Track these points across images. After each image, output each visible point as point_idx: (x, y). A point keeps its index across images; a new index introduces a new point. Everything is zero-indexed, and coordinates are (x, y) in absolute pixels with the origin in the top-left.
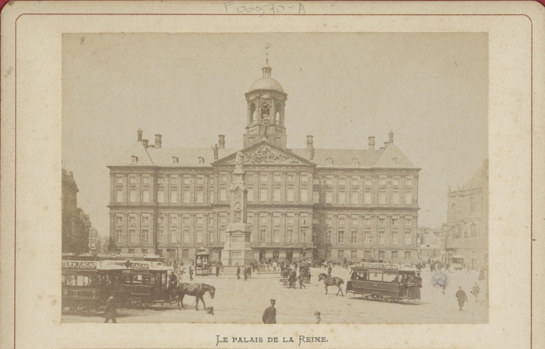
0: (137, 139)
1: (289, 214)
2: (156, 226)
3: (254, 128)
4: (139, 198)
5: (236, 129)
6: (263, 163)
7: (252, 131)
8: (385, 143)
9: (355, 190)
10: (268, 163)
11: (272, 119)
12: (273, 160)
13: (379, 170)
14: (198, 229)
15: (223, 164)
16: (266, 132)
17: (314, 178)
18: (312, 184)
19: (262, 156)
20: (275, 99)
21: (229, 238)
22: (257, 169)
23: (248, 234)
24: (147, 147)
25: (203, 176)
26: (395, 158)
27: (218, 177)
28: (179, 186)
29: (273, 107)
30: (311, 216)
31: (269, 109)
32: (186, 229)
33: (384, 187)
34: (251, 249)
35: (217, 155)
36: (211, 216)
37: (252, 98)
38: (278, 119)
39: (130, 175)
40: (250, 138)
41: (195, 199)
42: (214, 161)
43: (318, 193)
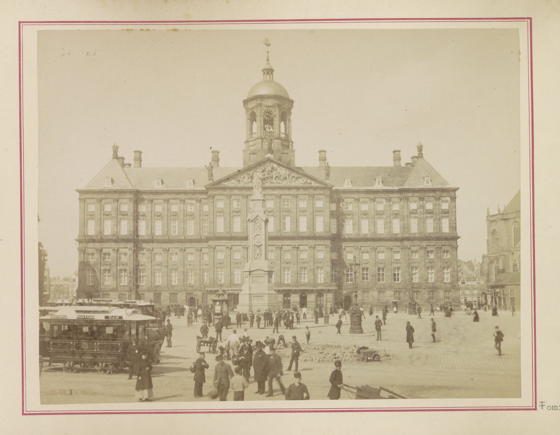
0: (111, 156)
3: (255, 142)
7: (253, 146)
9: (380, 216)
12: (280, 181)
13: (408, 191)
14: (189, 267)
15: (220, 186)
17: (332, 202)
18: (328, 211)
19: (266, 176)
20: (279, 106)
21: (247, 279)
23: (270, 273)
24: (123, 165)
25: (194, 202)
27: (213, 202)
30: (329, 249)
32: (174, 267)
33: (414, 212)
34: (275, 292)
35: (212, 175)
37: (251, 105)
38: (283, 130)
39: (104, 201)
42: (208, 182)
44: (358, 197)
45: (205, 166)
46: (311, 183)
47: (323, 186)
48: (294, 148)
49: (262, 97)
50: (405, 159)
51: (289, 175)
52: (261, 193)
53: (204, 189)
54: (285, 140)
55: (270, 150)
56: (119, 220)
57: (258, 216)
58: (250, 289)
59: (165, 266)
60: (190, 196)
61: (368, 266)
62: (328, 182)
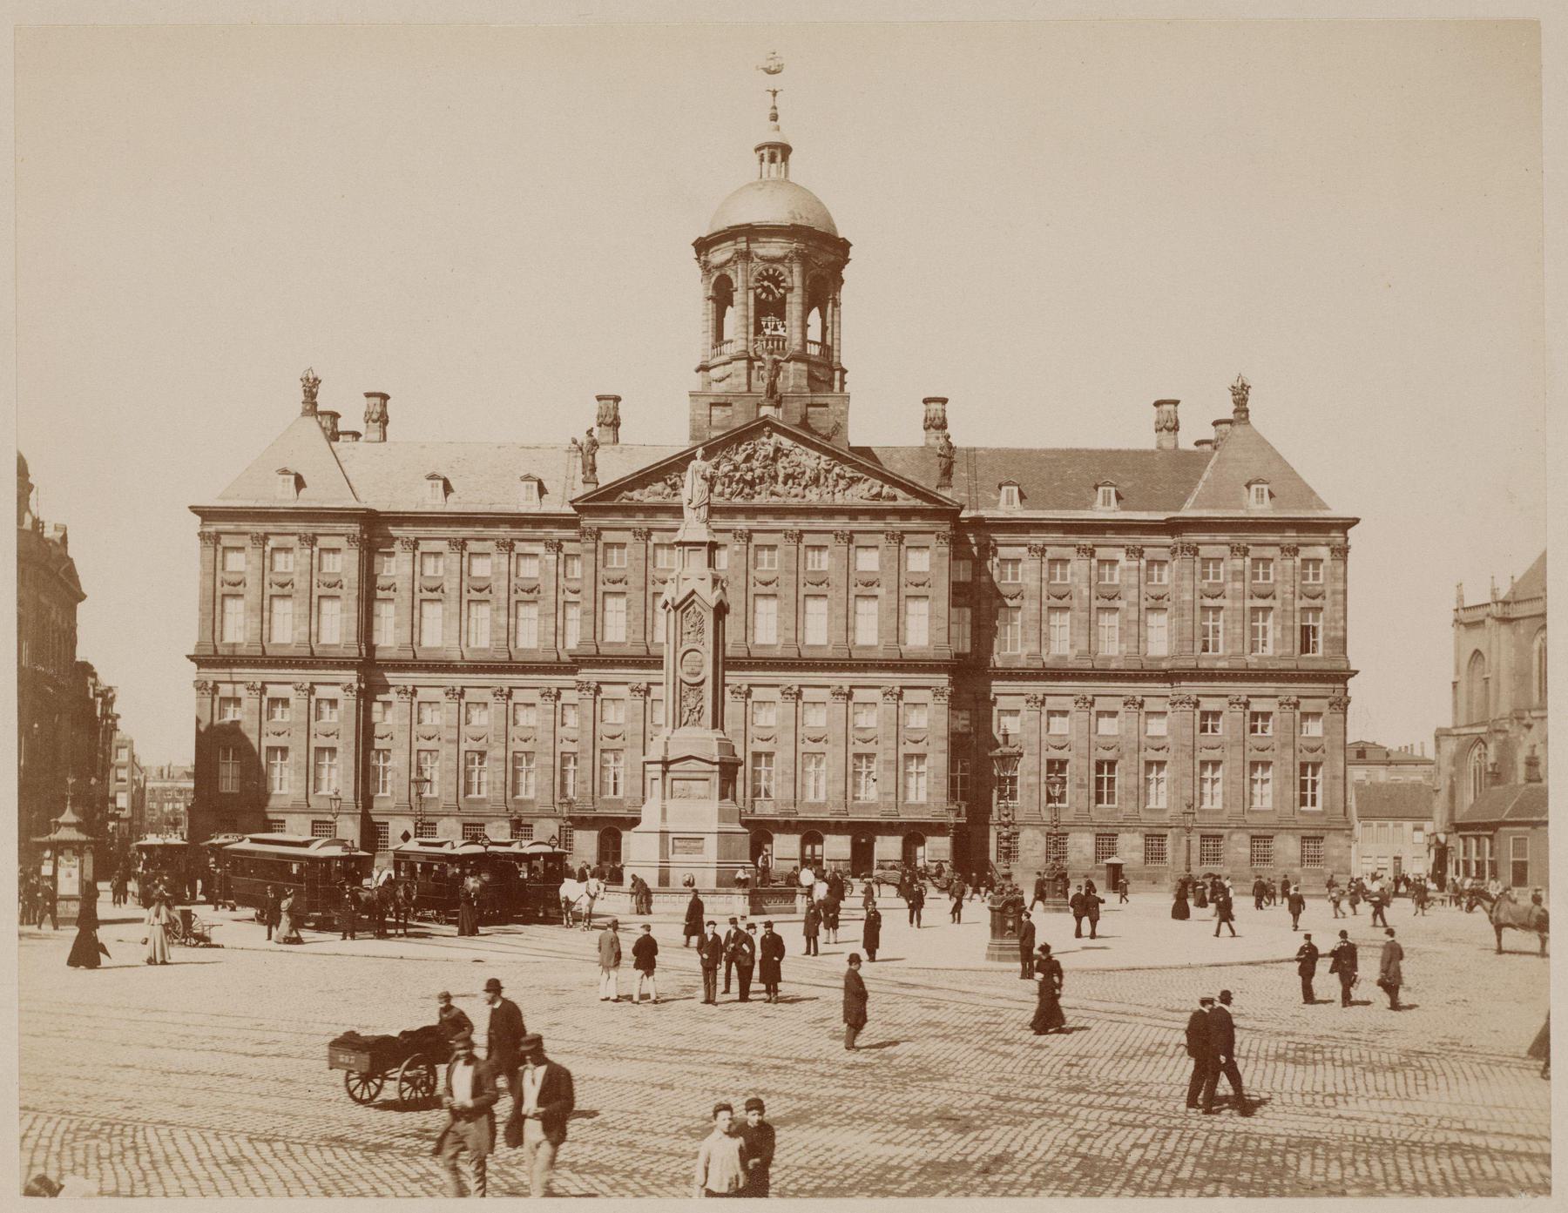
0: (299, 408)
1: (859, 695)
2: (366, 733)
5: (665, 377)
6: (758, 501)
7: (721, 380)
8: (1216, 424)
15: (615, 502)
19: (758, 472)
22: (742, 524)
25: (539, 549)
28: (451, 585)
29: (798, 291)
30: (944, 700)
35: (594, 470)
36: (567, 696)
38: (814, 333)
39: (273, 542)
41: (511, 633)
42: (581, 490)
43: (968, 612)
44: (1040, 542)
45: (575, 442)
46: (894, 498)
49: (752, 232)
51: (828, 471)
52: (707, 521)
54: (818, 365)
56: (315, 600)
57: (693, 592)
59: (449, 741)
60: (527, 531)
62: (947, 493)
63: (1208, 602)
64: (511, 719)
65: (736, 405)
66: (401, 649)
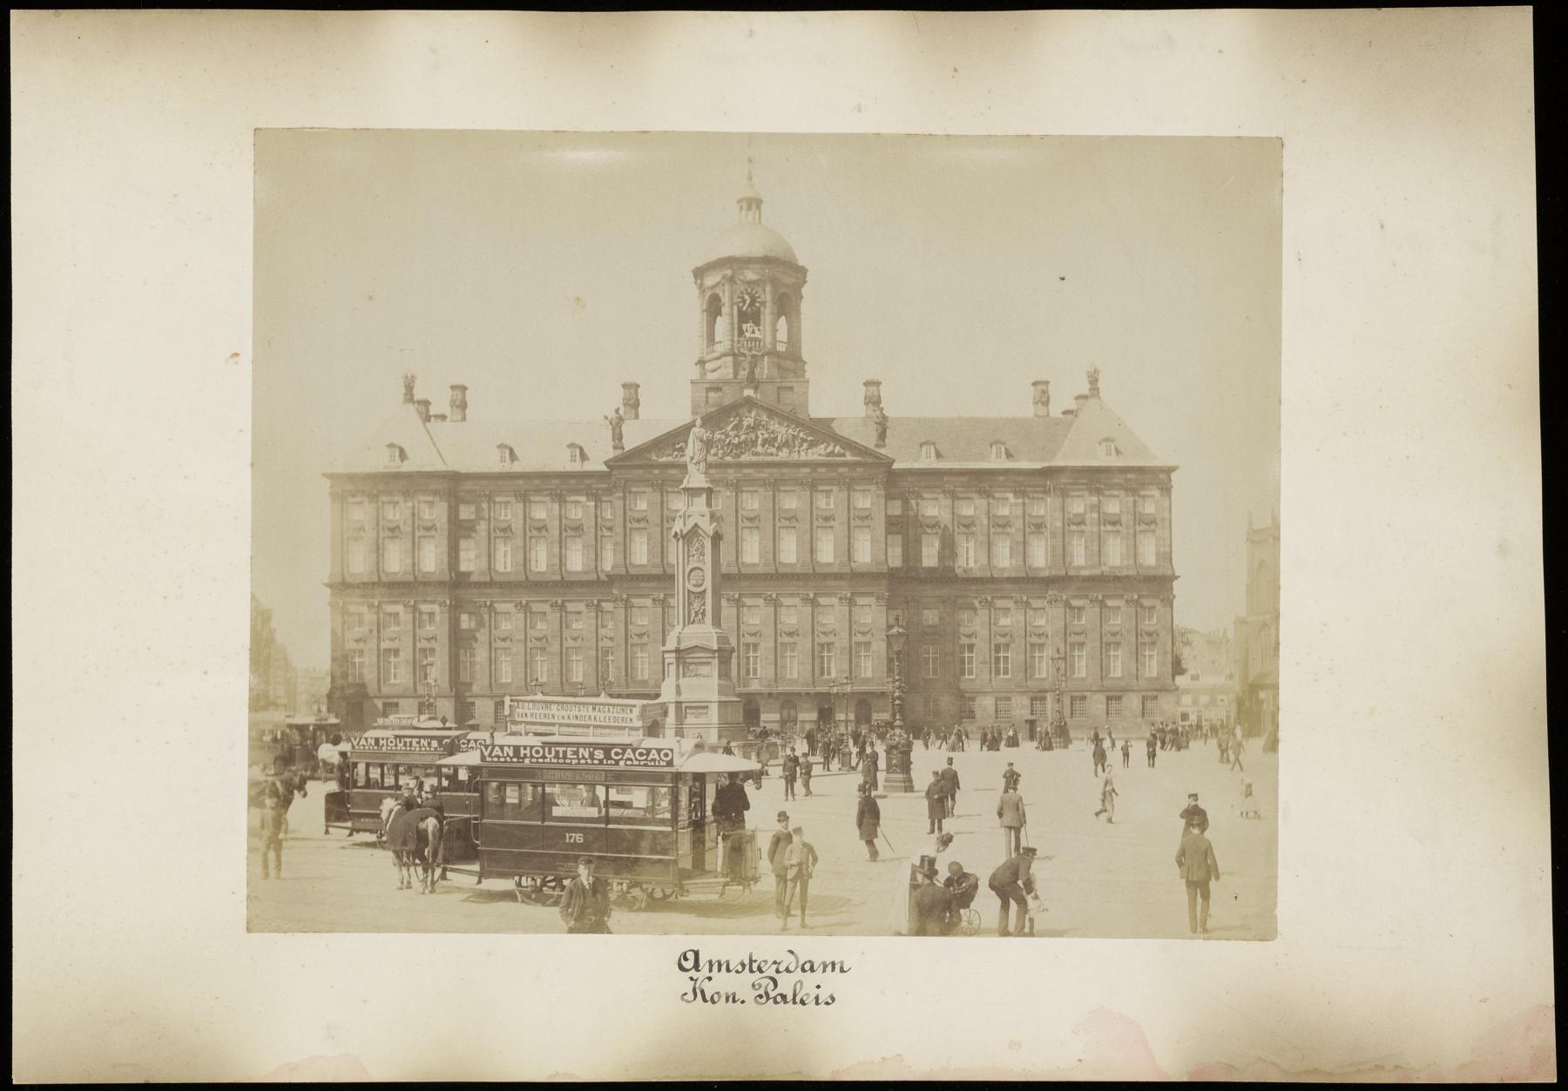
3: (719, 362)
4: (409, 561)
6: (746, 458)
8: (1078, 398)
10: (760, 459)
11: (769, 339)
12: (774, 450)
16: (752, 372)
20: (774, 282)
22: (731, 474)
24: (427, 418)
25: (583, 499)
26: (1107, 440)
27: (624, 498)
28: (517, 526)
29: (769, 305)
31: (759, 311)
37: (710, 280)
38: (782, 335)
40: (708, 390)
41: (562, 563)
42: (611, 454)
43: (898, 539)
47: (871, 460)
48: (807, 375)
50: (1061, 402)
53: (604, 468)
55: (753, 382)
57: (696, 525)
58: (678, 692)
61: (973, 640)
62: (882, 451)
63: (1074, 528)
64: (563, 624)
65: (726, 389)
66: (482, 573)
